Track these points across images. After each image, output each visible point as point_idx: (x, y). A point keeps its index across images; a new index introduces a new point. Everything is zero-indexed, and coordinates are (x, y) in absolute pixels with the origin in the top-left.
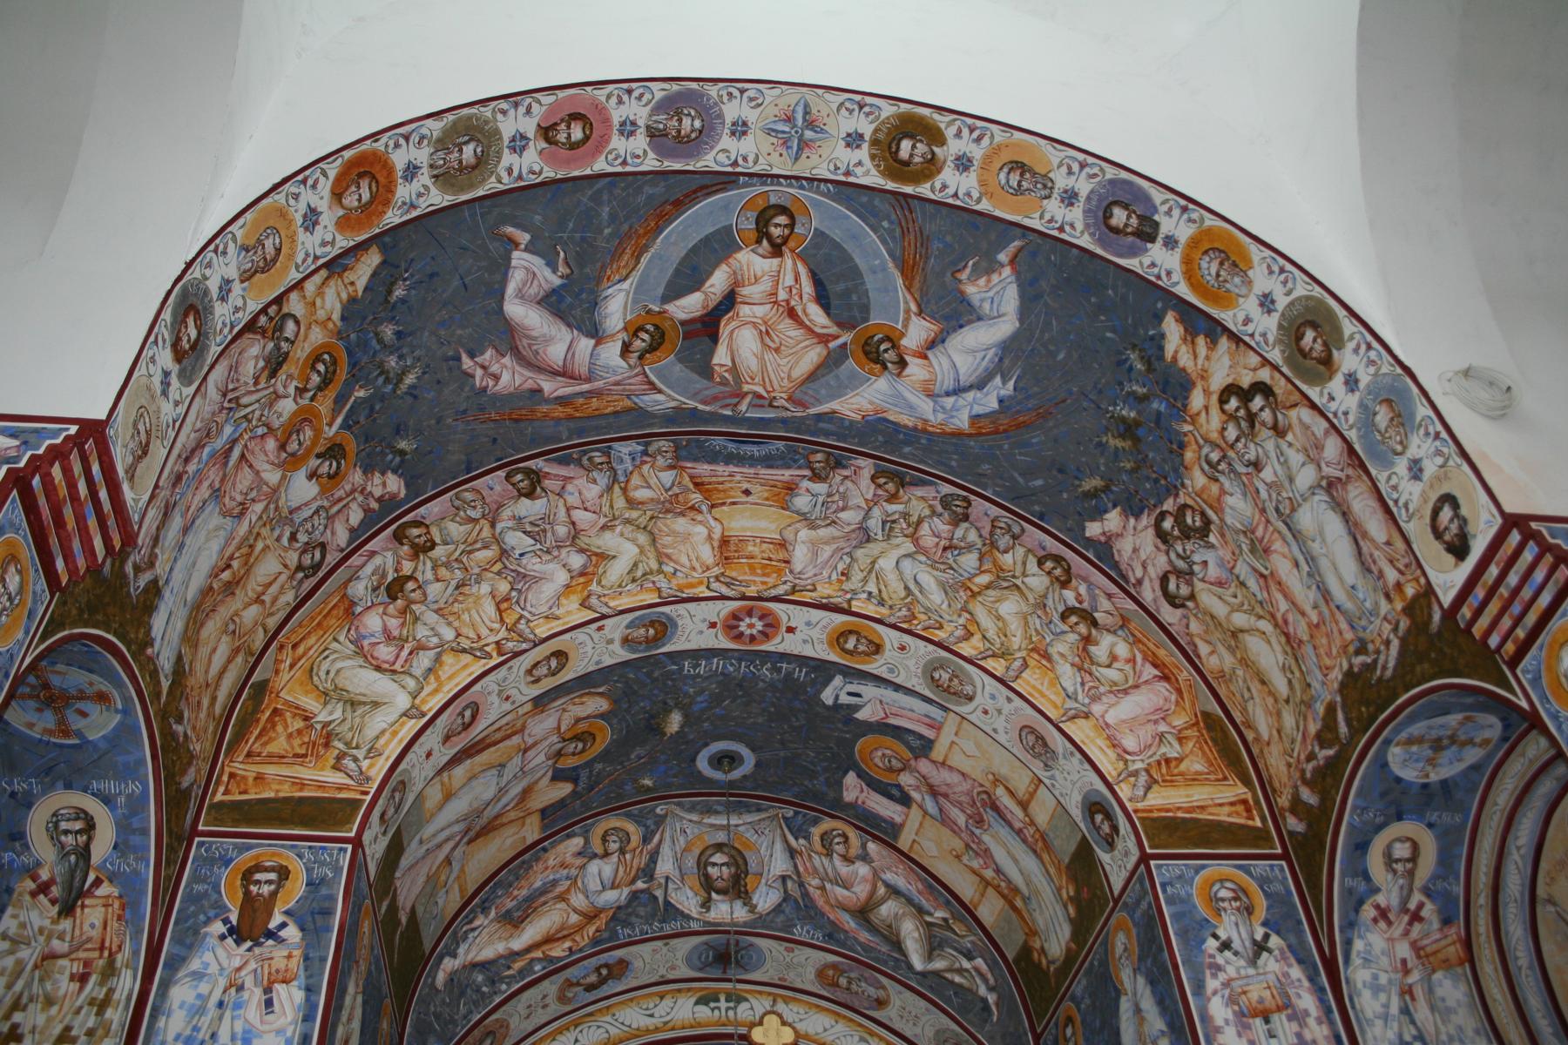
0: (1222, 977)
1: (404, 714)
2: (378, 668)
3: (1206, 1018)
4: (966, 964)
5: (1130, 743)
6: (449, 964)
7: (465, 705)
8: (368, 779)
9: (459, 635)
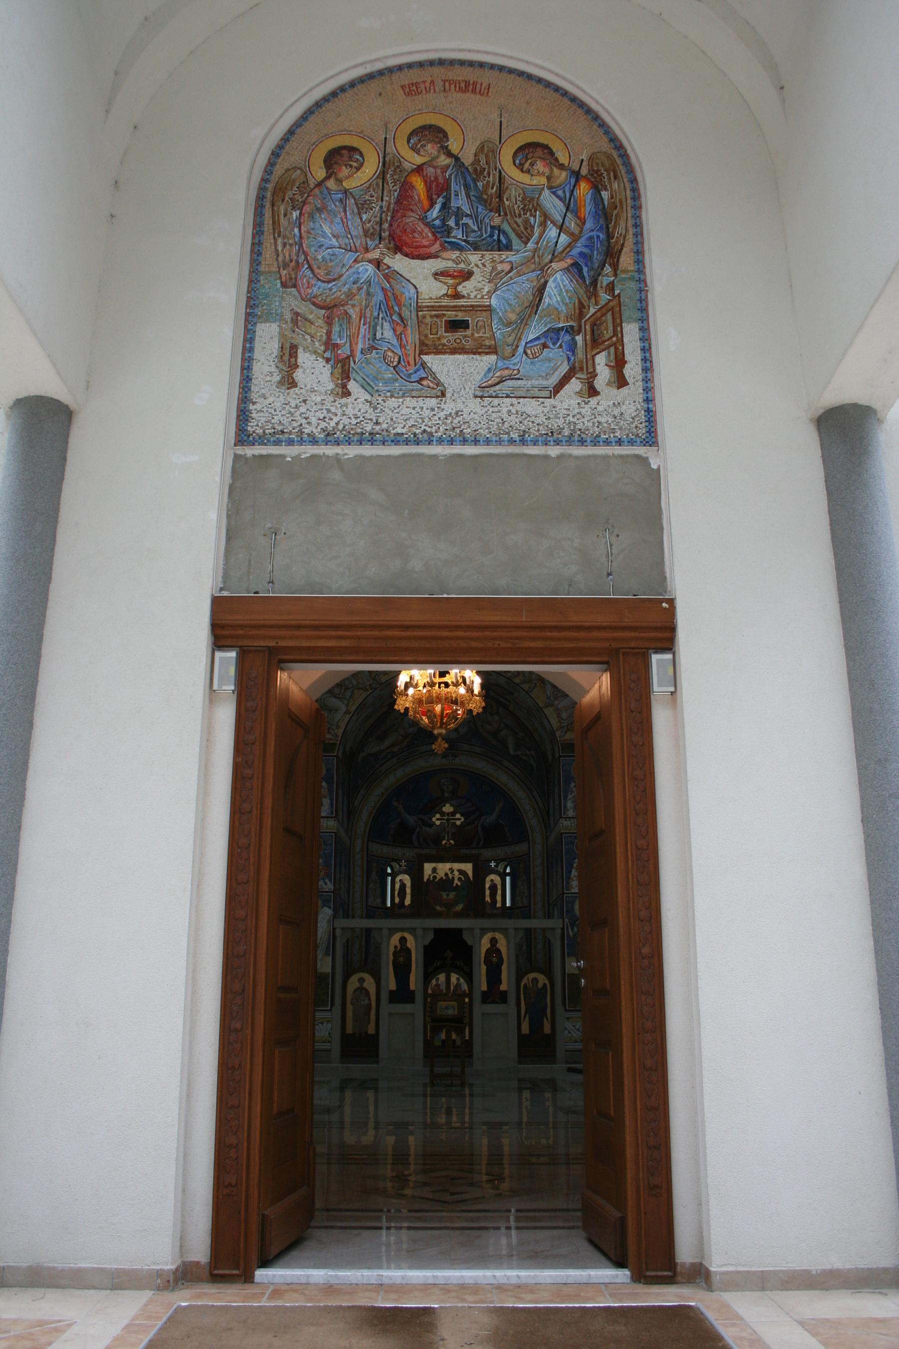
0: (573, 794)
1: (345, 713)
2: (335, 697)
3: (565, 806)
4: (528, 753)
5: (564, 715)
6: (362, 755)
7: (362, 706)
8: (337, 736)
9: (358, 683)
